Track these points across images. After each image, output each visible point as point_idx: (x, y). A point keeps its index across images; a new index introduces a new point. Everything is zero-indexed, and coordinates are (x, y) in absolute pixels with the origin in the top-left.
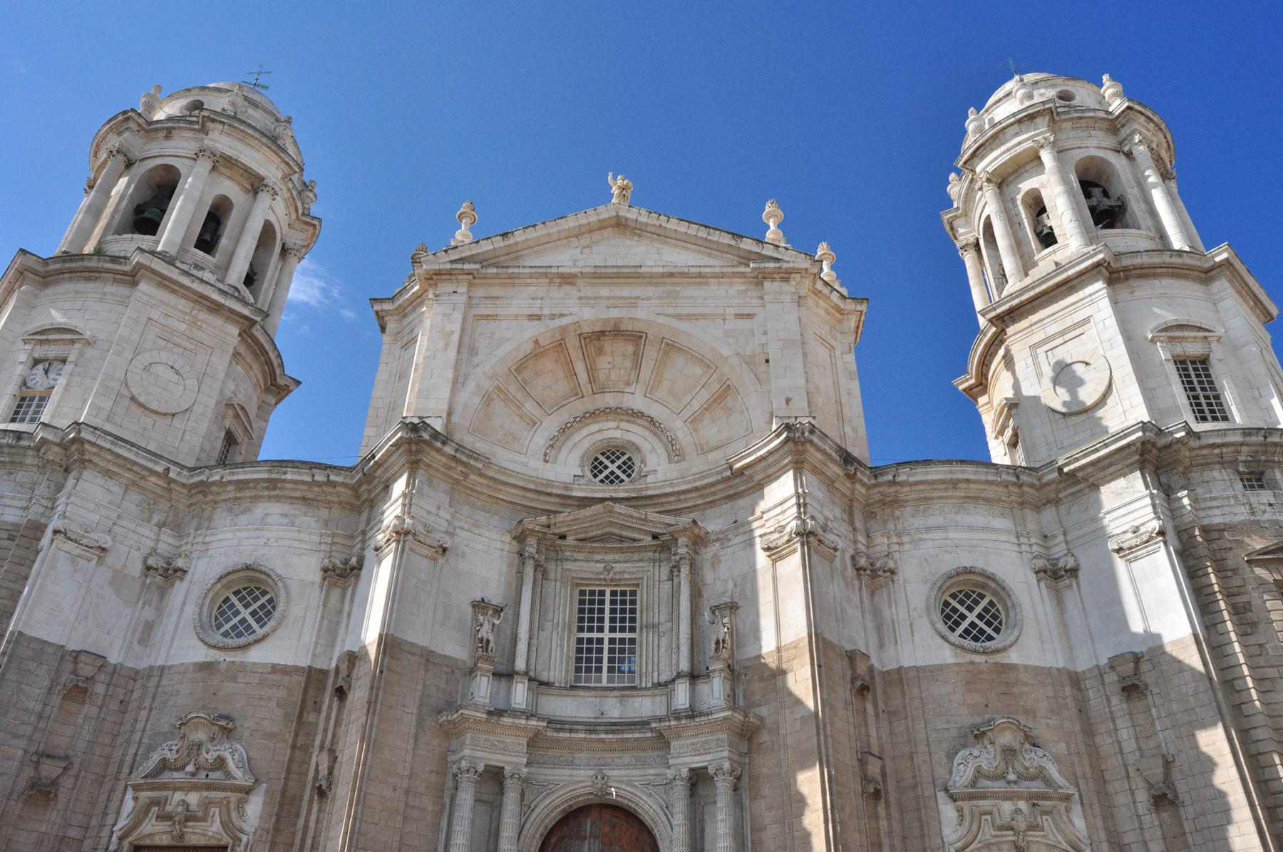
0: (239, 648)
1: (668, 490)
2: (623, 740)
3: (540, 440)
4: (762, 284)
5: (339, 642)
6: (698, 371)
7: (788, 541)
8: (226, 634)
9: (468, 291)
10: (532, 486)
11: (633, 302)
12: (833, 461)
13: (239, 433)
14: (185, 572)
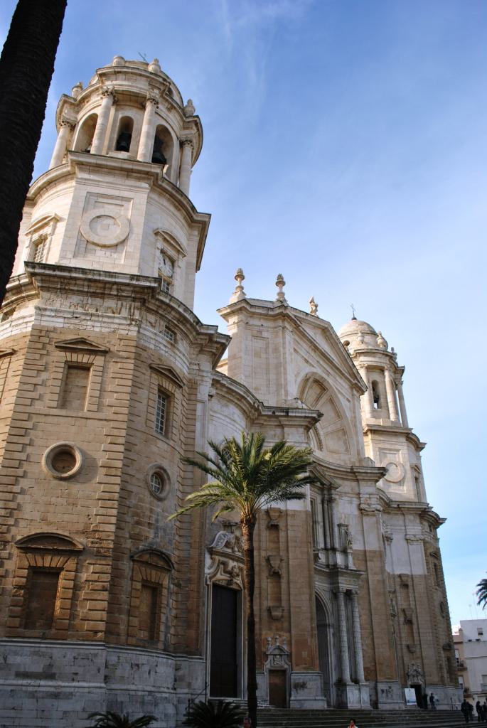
1: (327, 466)
6: (333, 415)
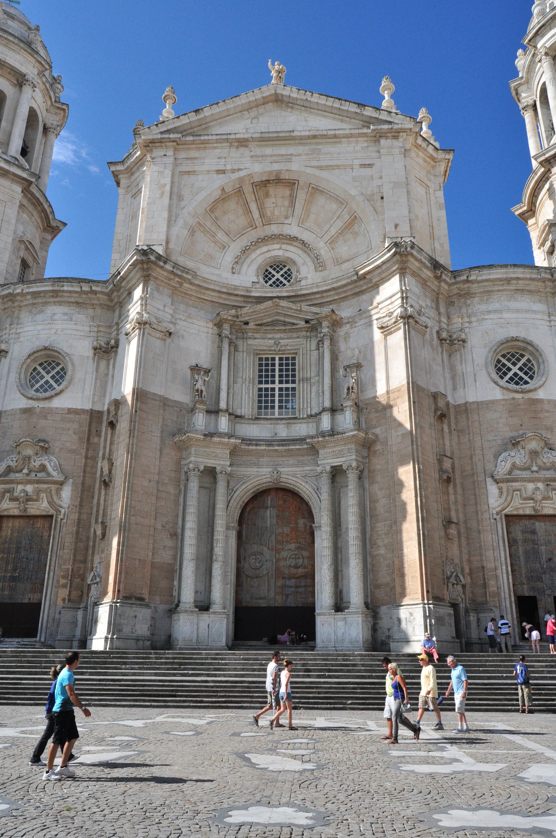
0: (46, 399)
1: (315, 290)
2: (289, 450)
3: (229, 258)
4: (379, 142)
5: (108, 394)
6: (334, 206)
7: (395, 322)
8: (37, 391)
9: (174, 154)
10: (224, 290)
11: (288, 158)
12: (427, 267)
13: (30, 260)
14: (7, 352)
